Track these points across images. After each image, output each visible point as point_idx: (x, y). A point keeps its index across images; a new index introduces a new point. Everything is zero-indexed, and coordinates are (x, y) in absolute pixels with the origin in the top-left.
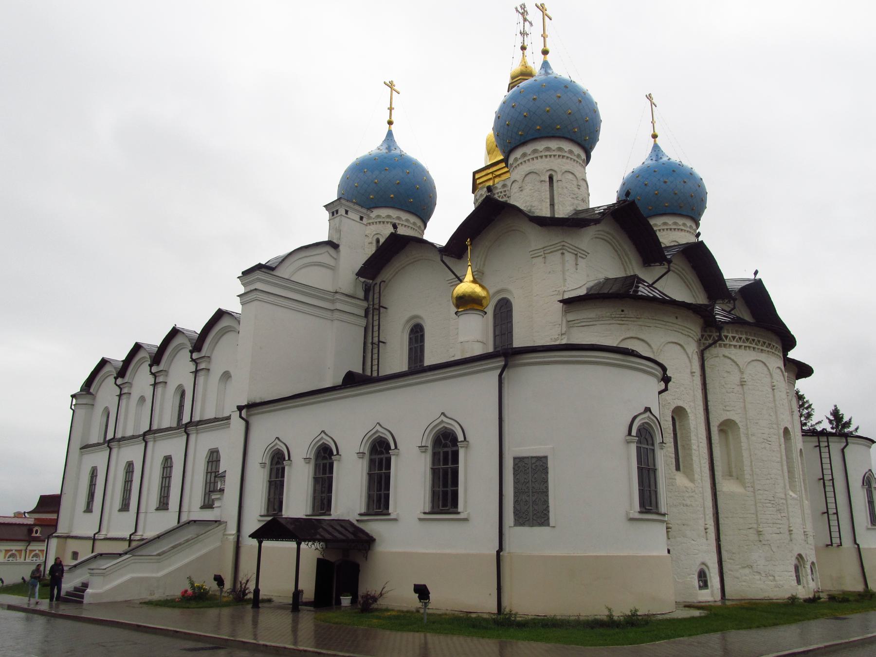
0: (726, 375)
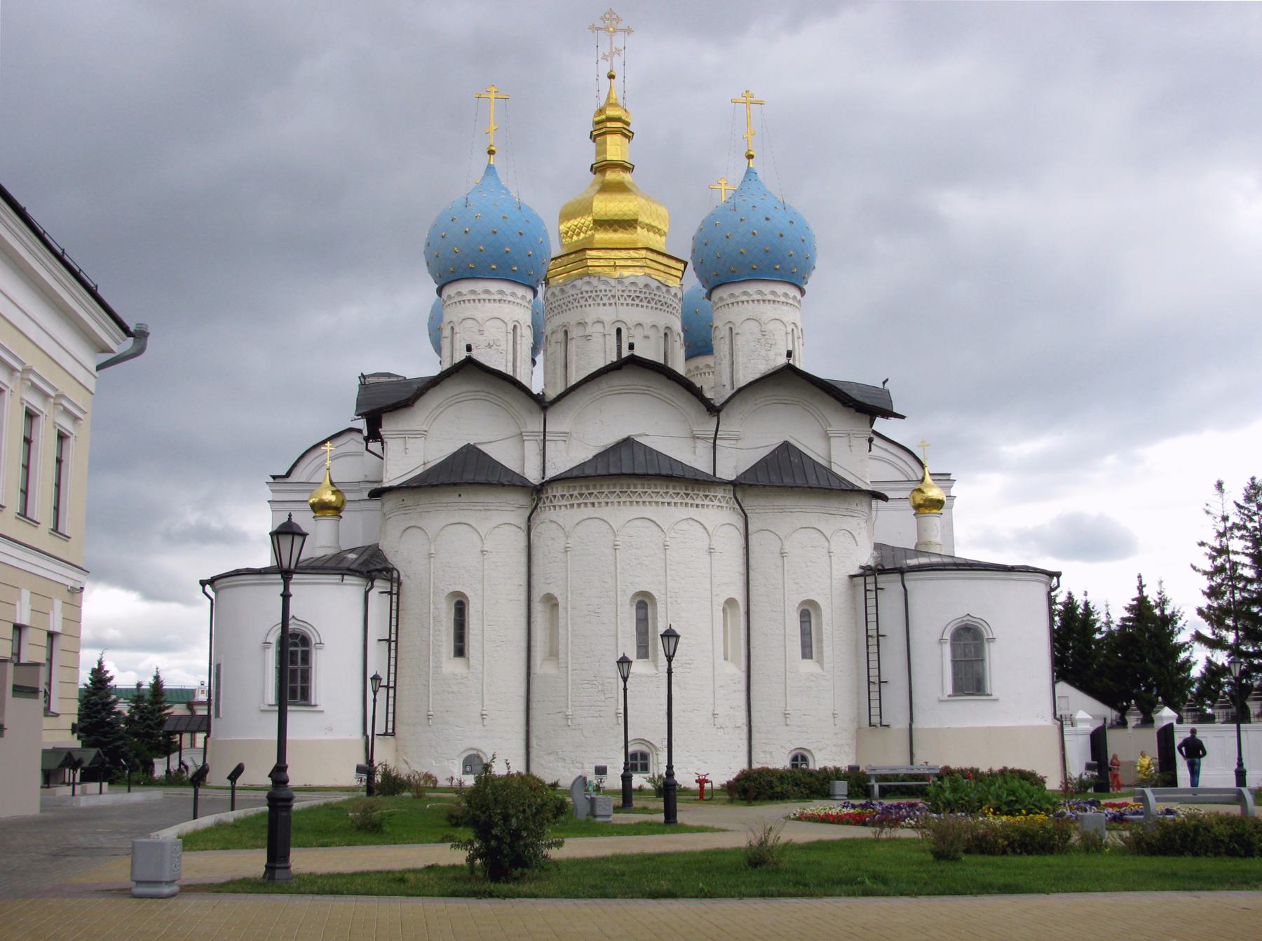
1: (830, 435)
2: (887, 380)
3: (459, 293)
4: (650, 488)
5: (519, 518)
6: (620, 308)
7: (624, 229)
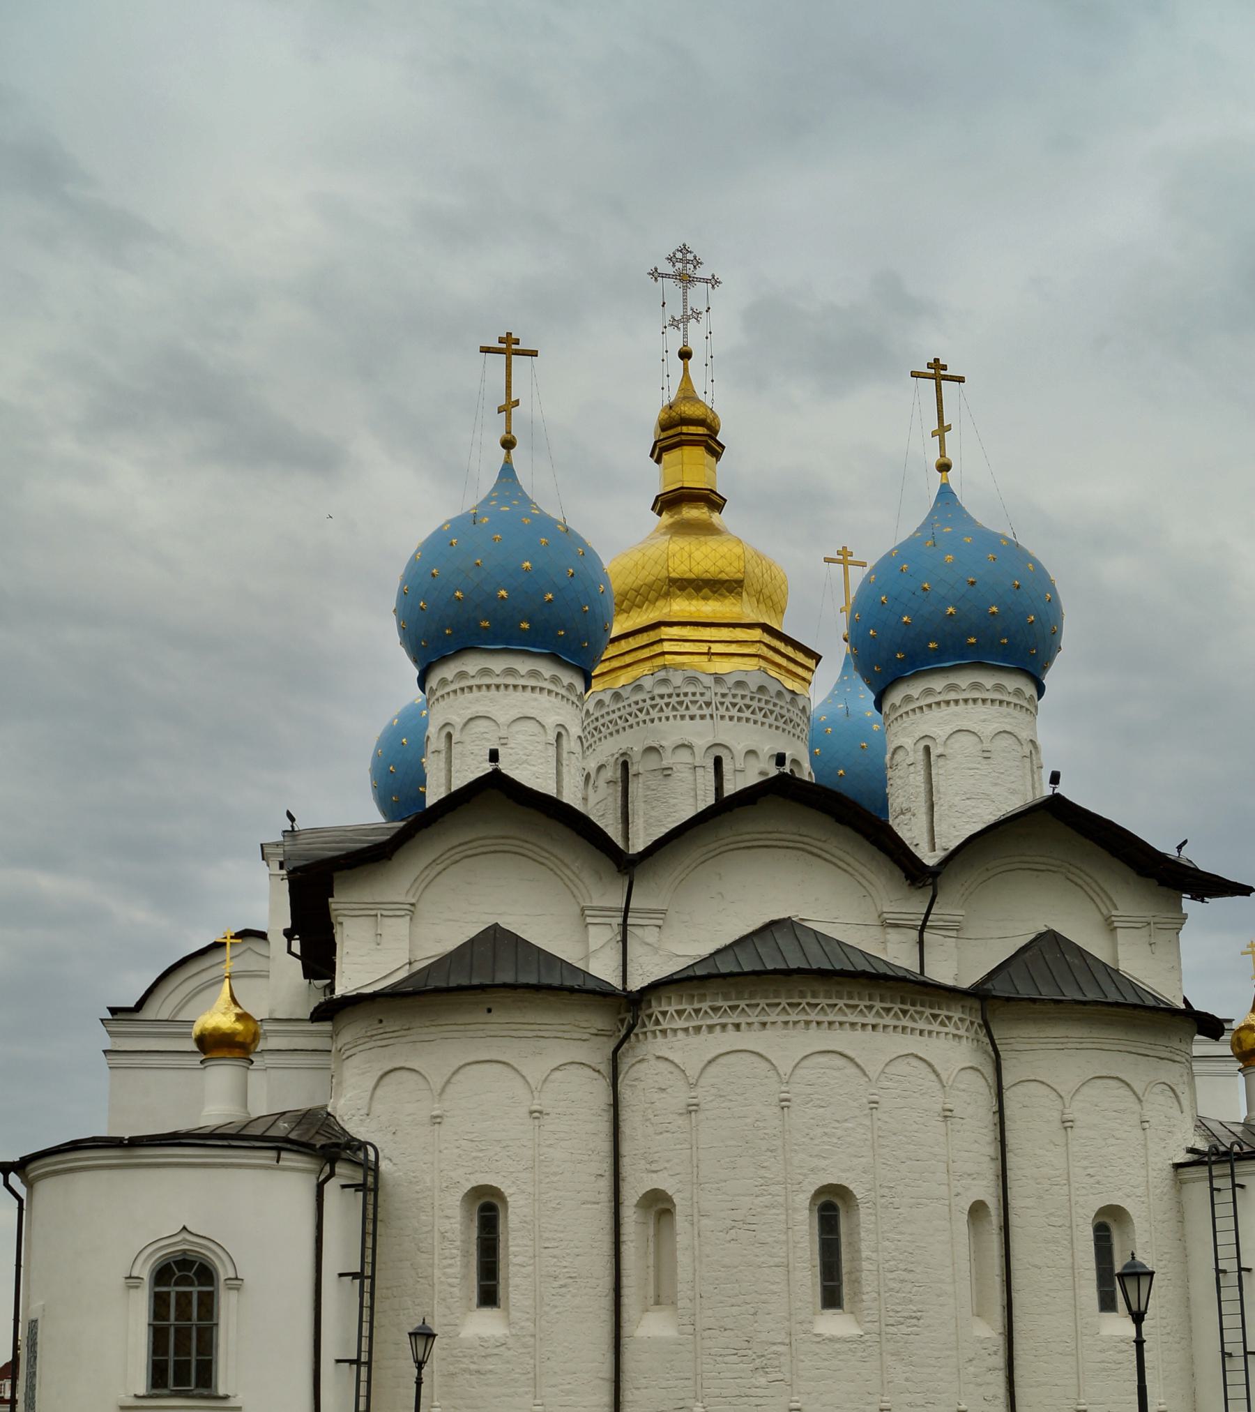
0: (656, 1096)
1: (1116, 924)
2: (1185, 842)
3: (462, 675)
4: (841, 998)
5: (599, 1054)
6: (717, 719)
7: (720, 595)
